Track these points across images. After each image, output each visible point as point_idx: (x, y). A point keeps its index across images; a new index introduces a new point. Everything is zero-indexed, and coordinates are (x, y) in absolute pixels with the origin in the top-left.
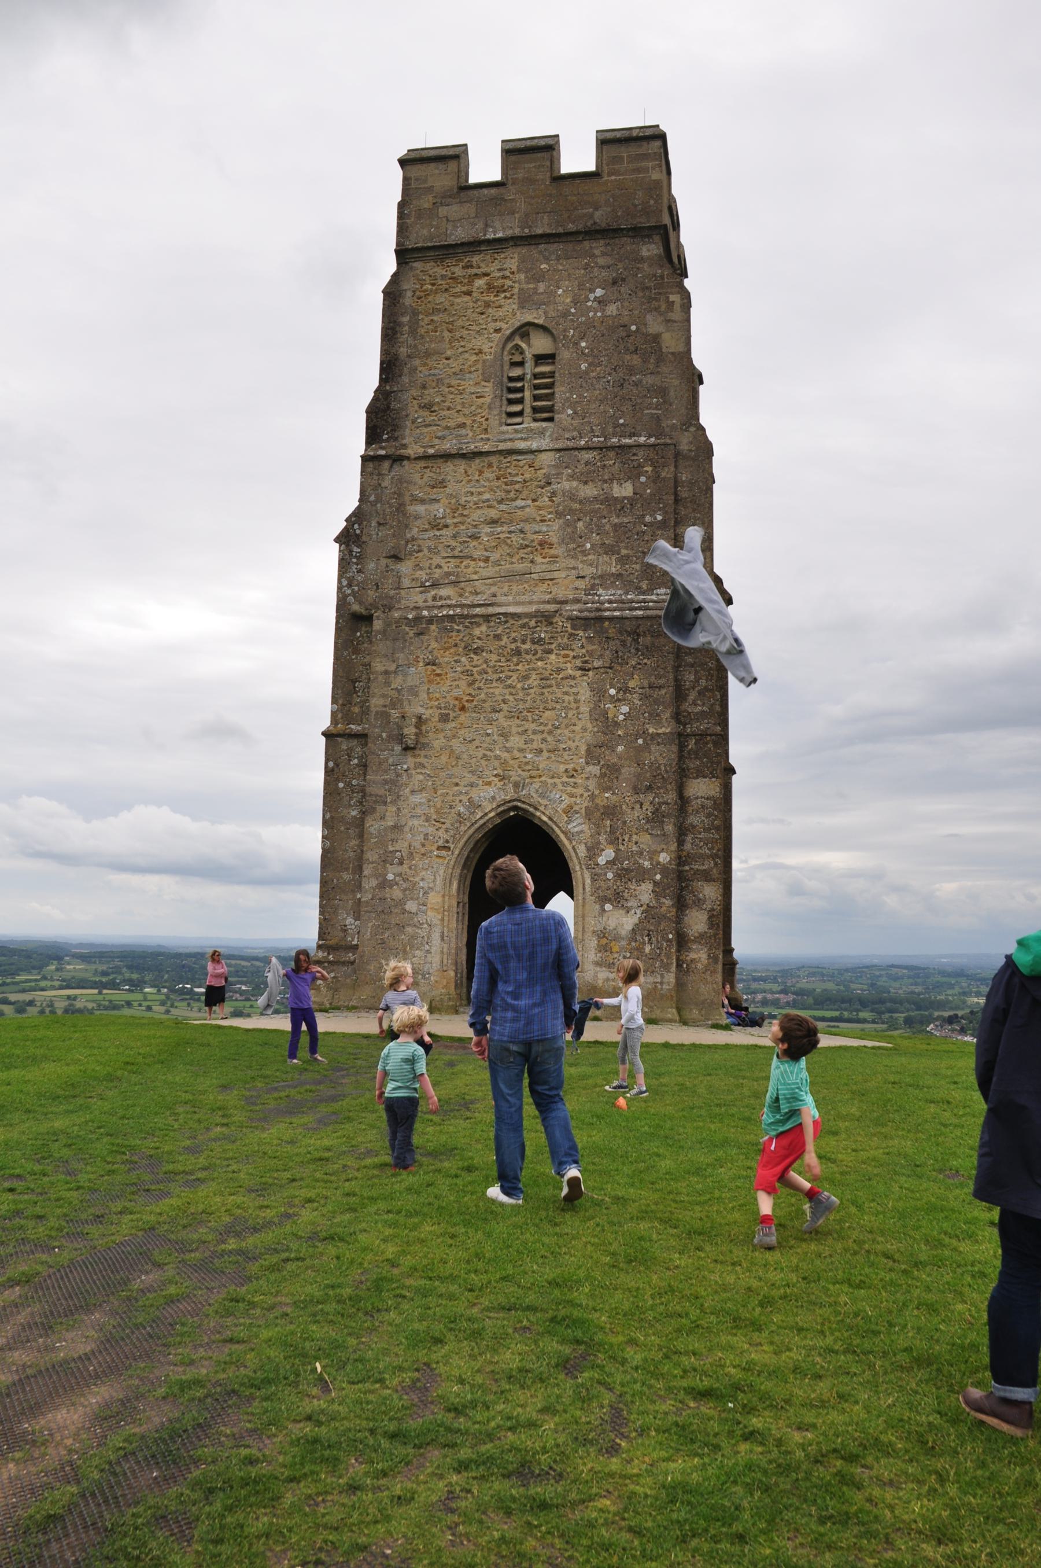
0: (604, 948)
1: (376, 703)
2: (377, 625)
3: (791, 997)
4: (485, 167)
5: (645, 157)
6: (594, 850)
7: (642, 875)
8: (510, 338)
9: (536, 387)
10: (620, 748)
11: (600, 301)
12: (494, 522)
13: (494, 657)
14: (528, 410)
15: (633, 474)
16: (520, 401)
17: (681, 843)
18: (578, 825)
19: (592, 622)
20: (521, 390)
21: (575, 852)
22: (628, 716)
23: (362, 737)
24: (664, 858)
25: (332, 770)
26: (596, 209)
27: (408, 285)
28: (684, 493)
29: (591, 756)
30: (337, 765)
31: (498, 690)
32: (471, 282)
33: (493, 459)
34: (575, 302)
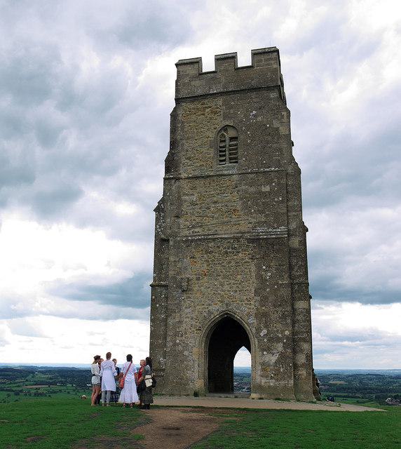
0: (263, 370)
1: (171, 273)
2: (171, 243)
3: (327, 387)
4: (209, 65)
5: (271, 59)
6: (259, 330)
7: (278, 340)
8: (220, 131)
9: (230, 150)
10: (268, 290)
11: (254, 115)
12: (215, 202)
13: (217, 255)
14: (228, 159)
15: (270, 183)
16: (225, 155)
17: (293, 327)
18: (252, 320)
19: (255, 240)
20: (225, 151)
21: (251, 331)
22: (271, 277)
23: (166, 286)
24: (287, 333)
25: (154, 299)
26: (253, 80)
27: (180, 112)
28: (290, 189)
29: (256, 293)
30: (156, 298)
31: (219, 268)
32: (204, 110)
33: (215, 178)
34: (245, 116)
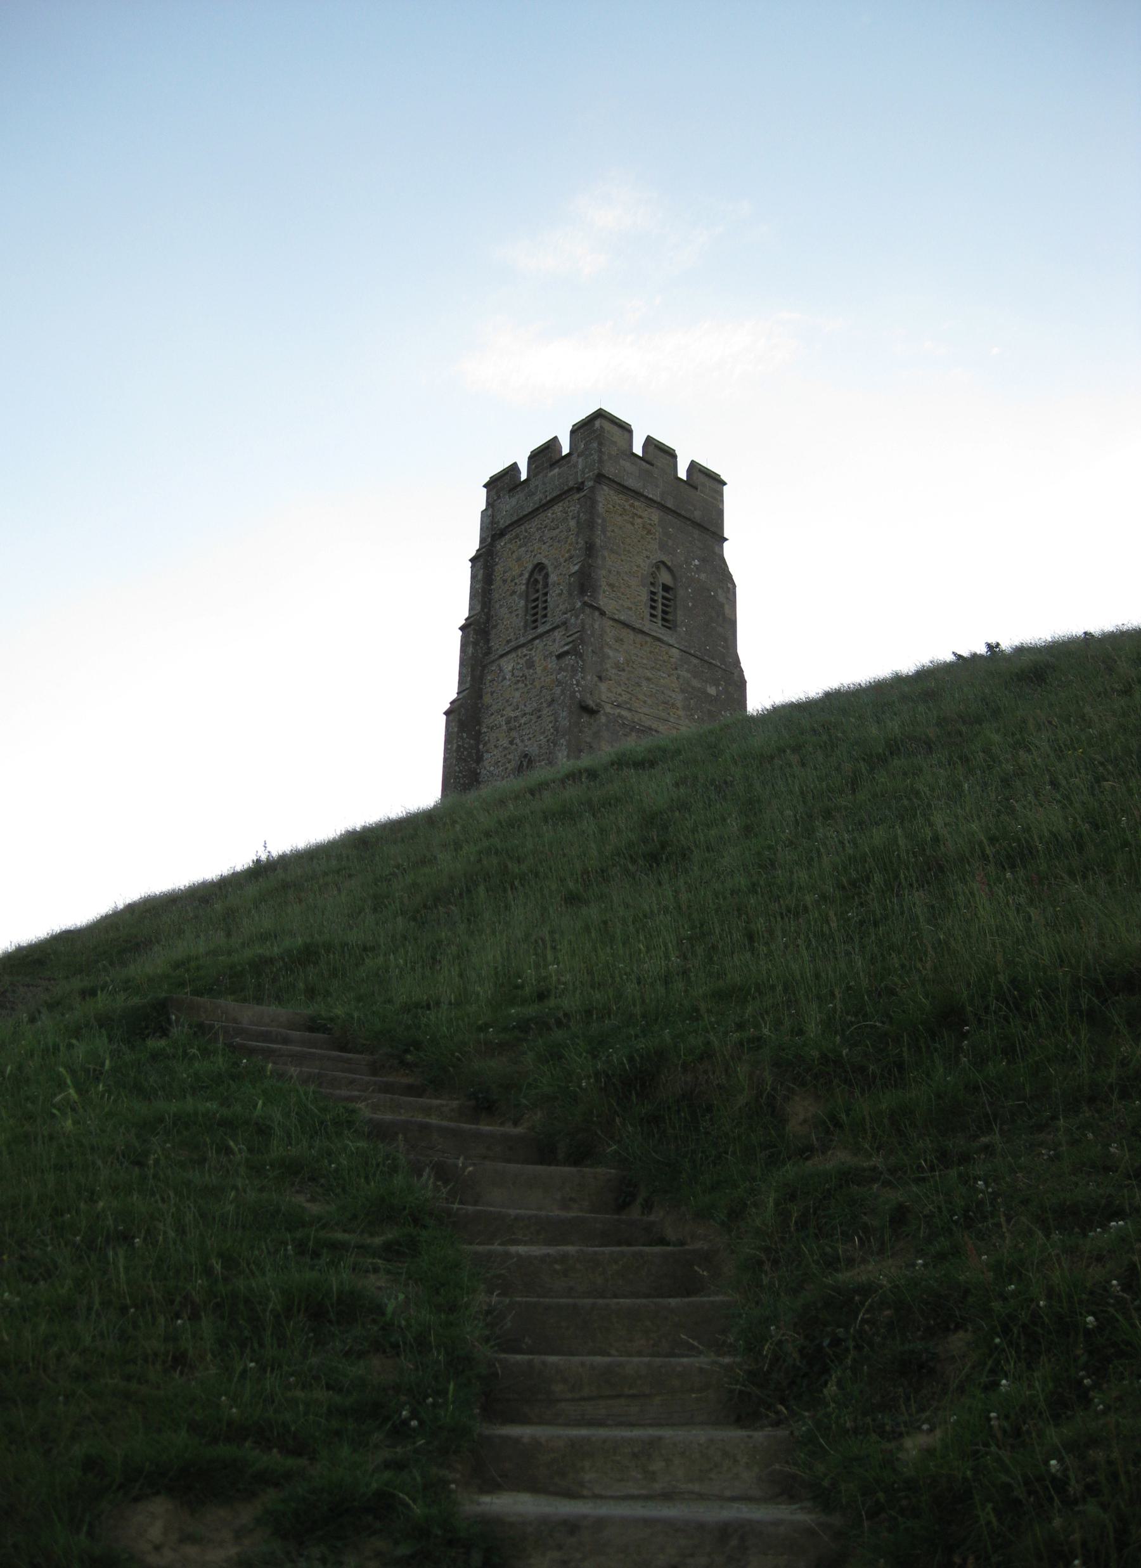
14: (660, 617)
